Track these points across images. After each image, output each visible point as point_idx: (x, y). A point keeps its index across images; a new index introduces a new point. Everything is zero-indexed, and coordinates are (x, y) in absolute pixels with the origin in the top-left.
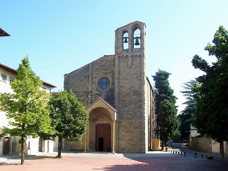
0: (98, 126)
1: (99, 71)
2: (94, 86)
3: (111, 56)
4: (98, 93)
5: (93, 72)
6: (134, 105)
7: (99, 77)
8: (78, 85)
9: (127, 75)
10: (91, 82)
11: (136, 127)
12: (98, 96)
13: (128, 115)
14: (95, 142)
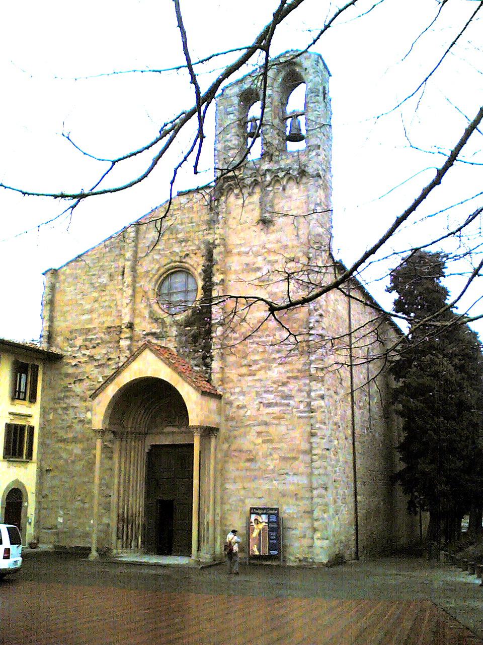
1: (159, 250)
2: (141, 306)
4: (153, 331)
6: (281, 369)
7: (160, 272)
9: (257, 255)
10: (130, 292)
12: (154, 341)
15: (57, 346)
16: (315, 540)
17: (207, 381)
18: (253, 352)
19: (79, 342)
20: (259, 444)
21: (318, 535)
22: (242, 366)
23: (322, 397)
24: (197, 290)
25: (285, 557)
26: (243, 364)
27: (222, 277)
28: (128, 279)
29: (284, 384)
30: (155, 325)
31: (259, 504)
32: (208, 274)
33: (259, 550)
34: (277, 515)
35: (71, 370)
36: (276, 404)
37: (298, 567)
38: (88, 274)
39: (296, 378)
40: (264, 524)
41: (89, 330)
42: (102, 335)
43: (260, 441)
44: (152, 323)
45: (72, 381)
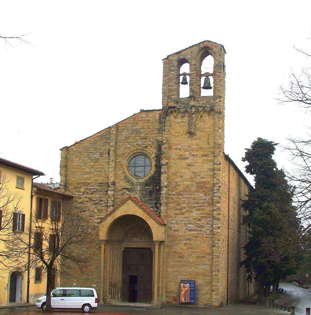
0: (127, 252)
3: (154, 112)
4: (127, 187)
5: (118, 144)
6: (197, 212)
8: (87, 170)
11: (202, 255)
12: (127, 192)
13: (187, 232)
14: (120, 285)
15: (70, 191)
16: (213, 295)
17: (158, 217)
18: (183, 203)
19: (82, 190)
20: (185, 250)
21: (214, 293)
22: (177, 209)
23: (219, 228)
24: (151, 166)
25: (197, 303)
26: (178, 208)
27: (167, 161)
28: (112, 157)
29: (199, 220)
30: (128, 184)
31: (184, 278)
32: (158, 158)
33: (185, 300)
34: (194, 284)
35: (78, 205)
36: (195, 230)
37: (205, 308)
38: (87, 152)
39: (205, 217)
40: (188, 288)
41: (89, 183)
42: (97, 187)
43: (186, 248)
44: (126, 182)
45: (79, 211)
